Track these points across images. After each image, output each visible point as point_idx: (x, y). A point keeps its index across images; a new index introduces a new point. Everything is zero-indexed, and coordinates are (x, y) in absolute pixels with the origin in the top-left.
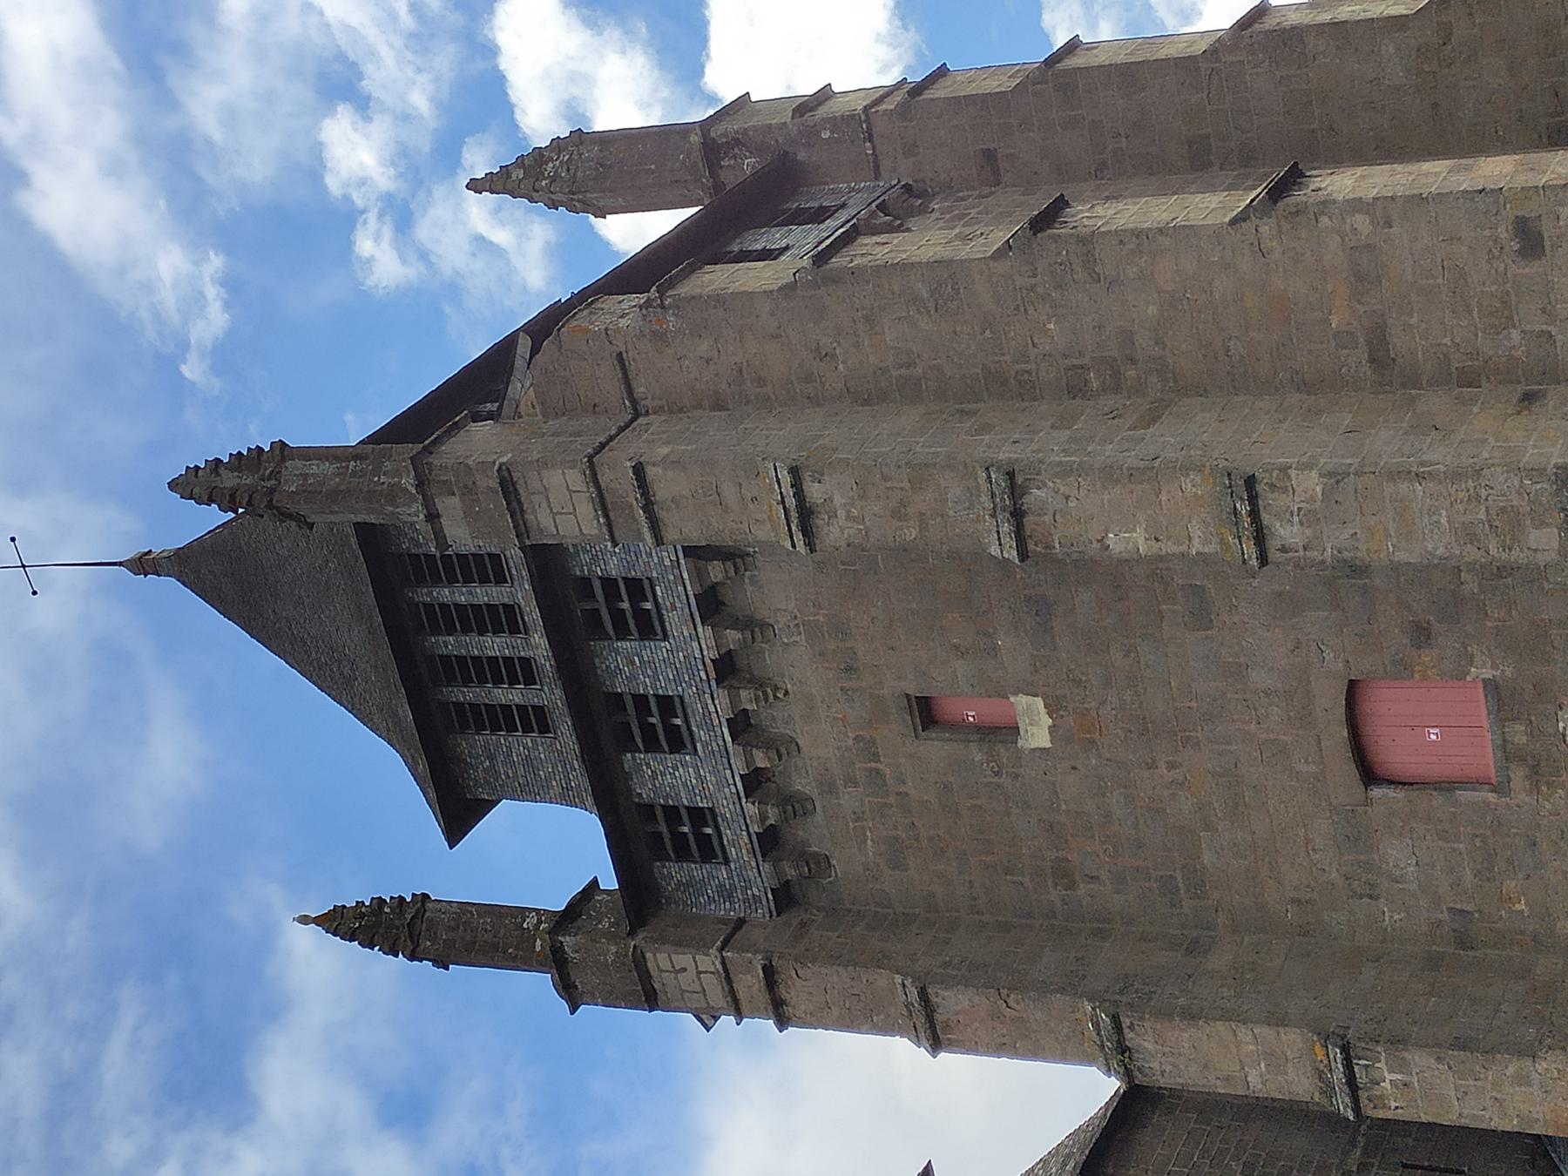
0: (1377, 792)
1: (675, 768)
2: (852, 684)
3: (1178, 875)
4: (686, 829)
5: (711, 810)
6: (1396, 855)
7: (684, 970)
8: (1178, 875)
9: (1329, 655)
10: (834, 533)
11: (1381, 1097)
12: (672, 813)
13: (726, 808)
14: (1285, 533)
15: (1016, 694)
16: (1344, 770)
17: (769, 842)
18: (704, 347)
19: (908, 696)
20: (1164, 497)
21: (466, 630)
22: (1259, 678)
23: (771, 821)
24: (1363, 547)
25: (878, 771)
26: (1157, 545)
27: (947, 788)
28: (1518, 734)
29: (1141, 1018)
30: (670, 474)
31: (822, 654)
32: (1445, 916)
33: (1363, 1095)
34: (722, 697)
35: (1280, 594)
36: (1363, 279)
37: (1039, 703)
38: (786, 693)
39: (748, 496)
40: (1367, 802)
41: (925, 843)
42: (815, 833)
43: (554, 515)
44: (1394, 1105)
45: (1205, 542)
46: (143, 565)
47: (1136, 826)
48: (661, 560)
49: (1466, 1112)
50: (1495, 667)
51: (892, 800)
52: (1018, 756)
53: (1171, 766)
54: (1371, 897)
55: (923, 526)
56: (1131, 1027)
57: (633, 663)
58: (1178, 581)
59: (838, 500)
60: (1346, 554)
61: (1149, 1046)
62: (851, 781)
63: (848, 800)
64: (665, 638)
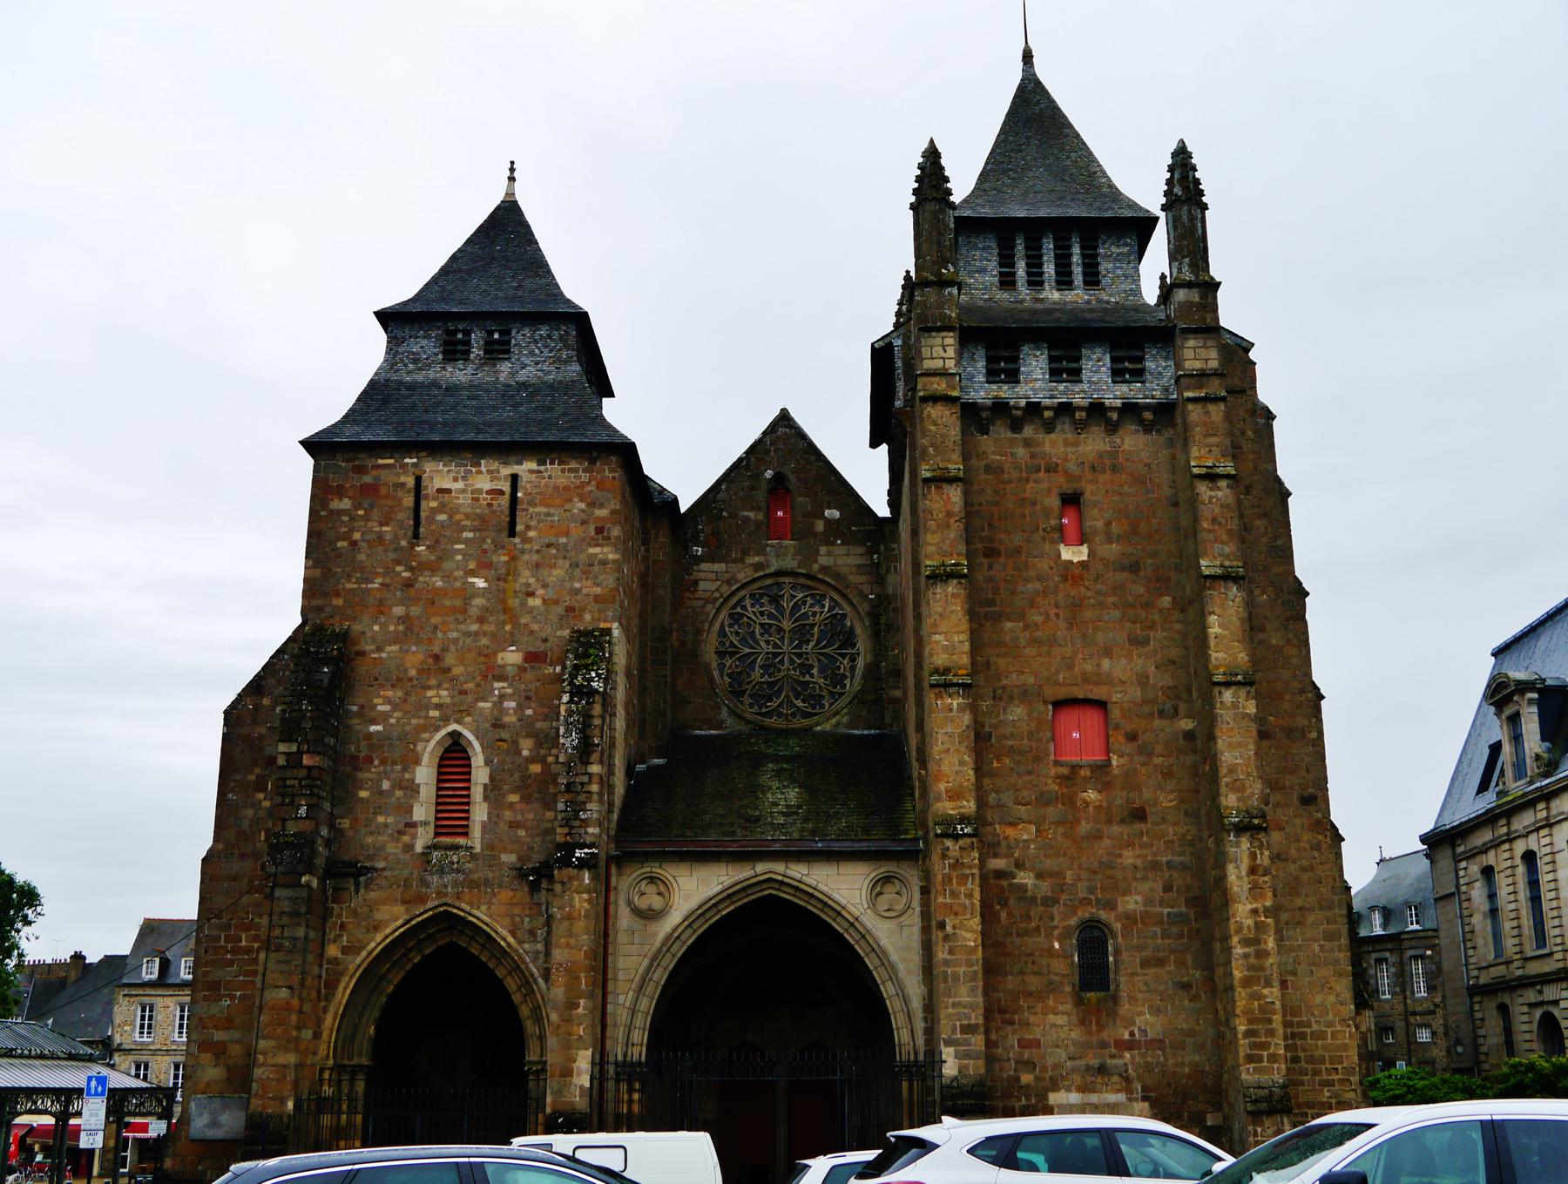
0: (1050, 707)
1: (1041, 369)
2: (1086, 468)
3: (997, 609)
4: (1002, 364)
5: (1018, 382)
6: (1017, 713)
7: (945, 351)
8: (997, 609)
9: (1119, 695)
10: (1202, 488)
11: (942, 697)
12: (1015, 359)
13: (1022, 389)
14: (1228, 695)
15: (1088, 547)
16: (1063, 693)
17: (1000, 408)
18: (1250, 433)
19: (1082, 494)
20: (1236, 644)
21: (1057, 257)
22: (1106, 663)
23: (1014, 412)
24: (1224, 726)
25: (1038, 470)
26: (1213, 636)
27: (1034, 504)
28: (1085, 773)
29: (965, 589)
30: (1221, 414)
31: (1101, 456)
32: (987, 729)
33: (943, 690)
34: (1085, 403)
35: (1148, 678)
36: (1289, 732)
37: (1085, 558)
38: (1079, 434)
39: (1213, 449)
40: (1045, 703)
41: (1002, 486)
42: (1001, 431)
43: (1194, 348)
44: (939, 703)
45: (1216, 659)
46: (1028, 57)
47: (1022, 592)
48: (1155, 390)
49: (940, 736)
50: (1117, 766)
51: (1024, 475)
52: (1058, 543)
53: (1057, 615)
54: (994, 698)
55: (1209, 531)
56: (959, 583)
57: (1099, 361)
58: (1152, 634)
59: (1219, 494)
60: (1219, 719)
61: (950, 590)
62: (1033, 456)
63: (1021, 452)
64: (1114, 382)
